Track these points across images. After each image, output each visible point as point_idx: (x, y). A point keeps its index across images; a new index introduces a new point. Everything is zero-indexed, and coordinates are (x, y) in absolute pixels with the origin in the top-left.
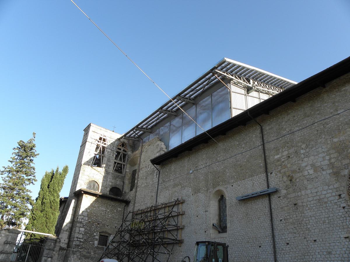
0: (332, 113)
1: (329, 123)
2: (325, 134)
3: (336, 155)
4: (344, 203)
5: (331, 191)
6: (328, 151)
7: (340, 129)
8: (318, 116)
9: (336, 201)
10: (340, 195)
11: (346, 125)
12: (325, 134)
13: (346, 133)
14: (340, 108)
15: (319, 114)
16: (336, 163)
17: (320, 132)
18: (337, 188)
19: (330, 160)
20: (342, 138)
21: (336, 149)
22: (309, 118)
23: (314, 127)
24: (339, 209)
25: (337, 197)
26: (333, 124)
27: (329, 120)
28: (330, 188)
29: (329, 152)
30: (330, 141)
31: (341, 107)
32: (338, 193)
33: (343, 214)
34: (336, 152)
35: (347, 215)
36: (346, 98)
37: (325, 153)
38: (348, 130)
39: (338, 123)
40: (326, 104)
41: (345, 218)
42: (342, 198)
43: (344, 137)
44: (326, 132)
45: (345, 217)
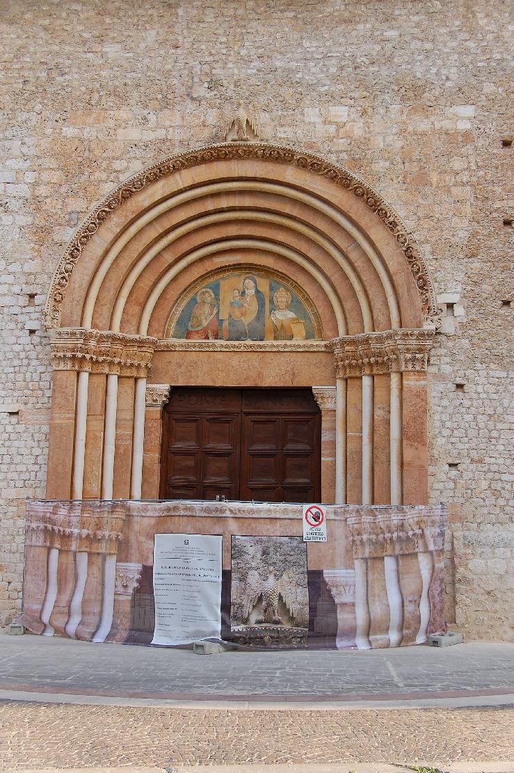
0: (85, 42)
3: (56, 177)
5: (10, 279)
8: (42, 34)
9: (16, 310)
10: (32, 296)
11: (112, 98)
13: (104, 122)
14: (114, 38)
15: (45, 29)
16: (48, 201)
17: (34, 89)
18: (30, 274)
19: (35, 184)
20: (90, 133)
22: (13, 28)
23: (18, 66)
24: (17, 332)
25: (23, 300)
28: (12, 268)
29: (40, 162)
31: (115, 35)
32: (29, 290)
34: (58, 169)
35: (33, 355)
36: (140, 12)
37: (28, 161)
40: (79, 8)
41: (25, 362)
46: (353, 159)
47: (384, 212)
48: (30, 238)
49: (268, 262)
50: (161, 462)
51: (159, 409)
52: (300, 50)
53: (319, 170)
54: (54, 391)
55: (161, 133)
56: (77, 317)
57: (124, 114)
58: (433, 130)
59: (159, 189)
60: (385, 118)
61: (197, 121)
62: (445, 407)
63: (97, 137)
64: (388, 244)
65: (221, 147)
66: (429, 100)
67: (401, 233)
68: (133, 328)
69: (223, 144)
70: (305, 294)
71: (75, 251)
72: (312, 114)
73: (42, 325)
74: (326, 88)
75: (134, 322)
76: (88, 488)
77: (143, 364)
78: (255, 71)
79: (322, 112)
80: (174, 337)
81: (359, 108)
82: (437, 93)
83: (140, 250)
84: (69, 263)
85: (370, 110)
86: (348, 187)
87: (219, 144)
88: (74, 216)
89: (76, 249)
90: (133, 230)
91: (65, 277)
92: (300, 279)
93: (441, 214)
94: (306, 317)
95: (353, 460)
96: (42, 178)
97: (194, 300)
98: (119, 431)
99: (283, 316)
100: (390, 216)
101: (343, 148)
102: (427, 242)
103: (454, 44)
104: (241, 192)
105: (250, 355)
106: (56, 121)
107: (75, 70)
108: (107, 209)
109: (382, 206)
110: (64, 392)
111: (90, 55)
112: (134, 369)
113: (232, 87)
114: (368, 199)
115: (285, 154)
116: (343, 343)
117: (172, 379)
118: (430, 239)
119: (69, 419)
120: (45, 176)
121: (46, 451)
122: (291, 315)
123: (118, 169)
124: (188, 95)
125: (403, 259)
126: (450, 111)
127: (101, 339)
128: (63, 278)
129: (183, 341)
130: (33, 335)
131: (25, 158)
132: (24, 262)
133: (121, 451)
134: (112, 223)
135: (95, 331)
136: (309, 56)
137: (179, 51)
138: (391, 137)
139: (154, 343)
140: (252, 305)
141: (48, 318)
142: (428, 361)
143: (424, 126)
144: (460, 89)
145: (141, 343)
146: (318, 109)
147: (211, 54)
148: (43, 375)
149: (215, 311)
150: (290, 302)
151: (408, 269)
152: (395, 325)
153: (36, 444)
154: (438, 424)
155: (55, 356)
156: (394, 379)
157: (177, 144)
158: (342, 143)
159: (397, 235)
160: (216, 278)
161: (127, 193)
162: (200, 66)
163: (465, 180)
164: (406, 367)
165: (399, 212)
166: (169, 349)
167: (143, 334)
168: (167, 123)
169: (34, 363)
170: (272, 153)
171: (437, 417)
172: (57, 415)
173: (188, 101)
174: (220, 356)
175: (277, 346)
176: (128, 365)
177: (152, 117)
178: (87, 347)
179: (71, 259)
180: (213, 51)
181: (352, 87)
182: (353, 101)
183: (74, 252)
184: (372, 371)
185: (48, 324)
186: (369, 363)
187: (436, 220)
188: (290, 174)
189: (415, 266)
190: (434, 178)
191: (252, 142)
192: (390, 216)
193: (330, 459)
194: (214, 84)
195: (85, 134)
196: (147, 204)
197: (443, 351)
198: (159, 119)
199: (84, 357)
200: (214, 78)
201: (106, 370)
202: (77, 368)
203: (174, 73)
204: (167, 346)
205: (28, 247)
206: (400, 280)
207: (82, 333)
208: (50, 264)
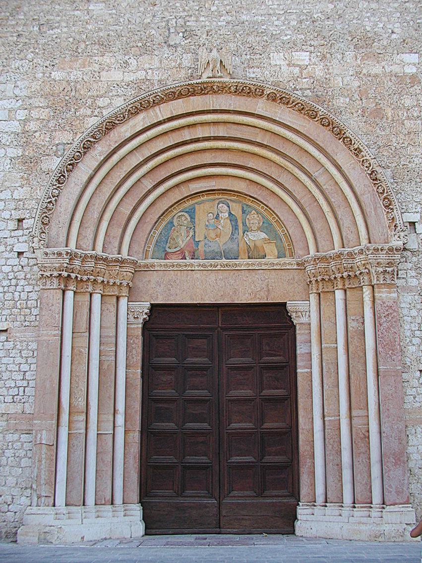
1: (57, 25)
2: (37, 51)
3: (45, 114)
6: (30, 98)
7: (80, 51)
10: (20, 221)
11: (97, 47)
12: (37, 51)
16: (37, 134)
17: (27, 41)
19: (26, 121)
20: (76, 75)
21: (52, 98)
25: (12, 225)
26: (65, 33)
27: (59, 18)
29: (31, 101)
30: (44, 73)
32: (17, 215)
37: (20, 101)
38: (96, 58)
39: (80, 33)
41: (14, 282)
43: (81, 73)
44: (40, 46)
45: (15, 278)
46: (317, 96)
47: (349, 139)
48: (20, 168)
49: (241, 186)
50: (142, 377)
51: (140, 326)
52: (263, 7)
53: (288, 103)
54: (41, 309)
55: (141, 75)
56: (62, 239)
57: (107, 59)
58: (385, 74)
59: (140, 121)
60: (341, 62)
61: (174, 64)
62: (414, 318)
63: (83, 79)
64: (354, 168)
65: (197, 83)
66: (379, 48)
67: (365, 158)
68: (115, 250)
69: (199, 81)
70: (275, 216)
71: (62, 177)
72: (278, 59)
74: (289, 37)
75: (117, 244)
76: (75, 403)
77: (125, 284)
78: (224, 23)
79: (286, 57)
81: (319, 54)
82: (385, 43)
83: (122, 177)
84: (56, 189)
85: (328, 55)
86: (315, 118)
87: (195, 82)
88: (61, 147)
89: (62, 175)
90: (116, 158)
91: (52, 201)
92: (272, 203)
93: (398, 144)
94: (276, 237)
95: (328, 370)
96: (32, 115)
97: (171, 223)
98: (102, 347)
99: (257, 237)
100: (354, 144)
101: (307, 86)
102: (388, 167)
103: (396, 5)
104: (216, 123)
105: (226, 274)
106: (46, 67)
107: (64, 24)
108: (92, 140)
109: (347, 134)
110: (50, 310)
111: (76, 13)
112: (116, 287)
113: (204, 36)
114: (334, 128)
115: (256, 90)
116: (317, 259)
117: (152, 297)
118: (390, 165)
119: (54, 336)
120: (35, 114)
121: (33, 367)
122: (263, 235)
123: (102, 106)
124: (165, 43)
125: (368, 181)
126: (397, 58)
127: (84, 258)
128: (51, 202)
129: (163, 262)
130: (21, 256)
131: (18, 98)
132: (14, 190)
133: (105, 367)
134: (96, 152)
135: (79, 252)
136: (271, 12)
137: (156, 8)
138: (348, 78)
139: (135, 263)
140: (225, 225)
141: (36, 240)
142: (397, 275)
143: (377, 70)
144: (404, 41)
145: (123, 261)
146: (283, 54)
147: (184, 10)
149: (191, 234)
150: (261, 223)
151: (373, 190)
152: (364, 242)
153: (24, 361)
154: (408, 333)
155: (42, 275)
156: (367, 292)
157: (156, 83)
158: (305, 83)
159: (362, 160)
160: (191, 202)
161: (110, 126)
162: (175, 20)
163: (415, 115)
164: (378, 280)
165: (361, 141)
166: (148, 268)
167: (125, 254)
168: (147, 66)
169: (22, 282)
170: (244, 88)
171: (407, 327)
172: (45, 332)
173: (166, 48)
174: (198, 275)
175: (253, 264)
177: (133, 62)
178: (72, 266)
179: (58, 185)
180: (187, 8)
181: (312, 37)
182: (313, 48)
183: (61, 179)
184: (344, 285)
185: (35, 245)
186: (342, 277)
187: (393, 149)
188: (261, 106)
189: (380, 187)
190: (389, 113)
191: (226, 79)
192: (354, 144)
193: (306, 370)
194: (188, 34)
195: (72, 77)
196: (128, 135)
197: (409, 265)
198: (139, 63)
199: (69, 276)
200: (188, 29)
201: (90, 290)
203: (153, 25)
204: (146, 266)
205: (18, 176)
206: (366, 199)
207: (67, 253)
208: (38, 191)
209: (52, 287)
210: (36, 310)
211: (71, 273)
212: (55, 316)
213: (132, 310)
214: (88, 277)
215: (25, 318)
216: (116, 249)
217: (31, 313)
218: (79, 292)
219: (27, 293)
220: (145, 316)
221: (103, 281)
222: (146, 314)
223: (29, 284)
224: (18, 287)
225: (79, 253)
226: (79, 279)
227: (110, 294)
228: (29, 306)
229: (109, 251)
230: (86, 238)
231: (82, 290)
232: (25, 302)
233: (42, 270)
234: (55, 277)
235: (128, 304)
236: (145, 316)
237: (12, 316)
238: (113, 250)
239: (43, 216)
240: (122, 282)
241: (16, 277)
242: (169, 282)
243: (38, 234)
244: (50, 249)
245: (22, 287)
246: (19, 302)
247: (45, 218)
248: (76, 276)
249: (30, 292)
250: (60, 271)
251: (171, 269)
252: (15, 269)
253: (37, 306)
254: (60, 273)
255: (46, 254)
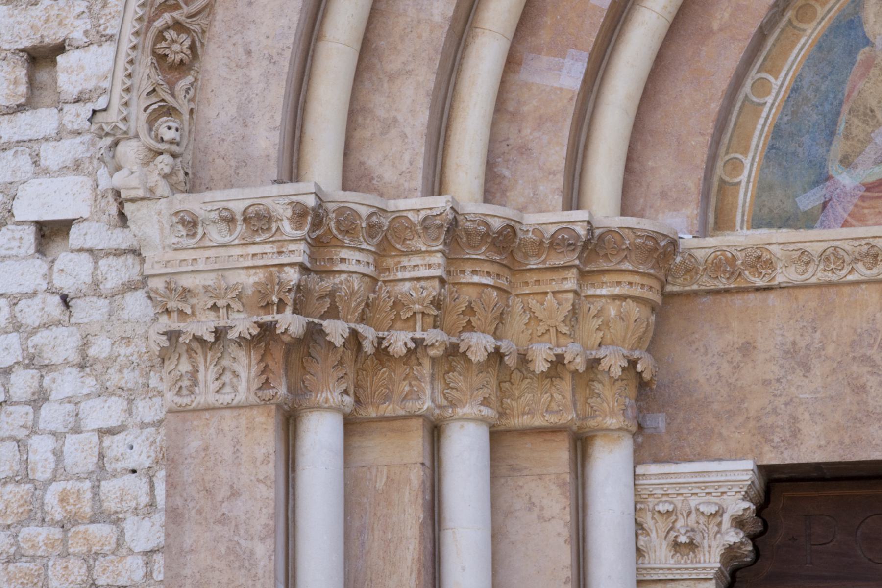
4: (77, 166)
33: (17, 327)
42: (59, 104)
45: (31, 361)
54: (174, 516)
73: (98, 196)
80: (757, 223)
110: (223, 520)
112: (566, 386)
117: (764, 433)
141: (129, 151)
148: (116, 445)
155: (173, 336)
176: (541, 366)
178: (328, 283)
199: (314, 333)
202: (282, 390)
209: (226, 398)
210: (147, 523)
211: (323, 317)
212: (252, 553)
213: (662, 508)
214: (419, 335)
215: (90, 569)
216: (559, 181)
217: (118, 545)
218: (371, 420)
219: (95, 438)
220: (734, 537)
221: (497, 355)
222: (739, 523)
223: (104, 392)
224: (46, 410)
225: (364, 211)
226: (368, 348)
227: (538, 422)
228: (111, 505)
229: (519, 193)
230: (394, 133)
231: (388, 409)
232: (87, 484)
233: (168, 312)
234: (241, 341)
235: (635, 476)
236: (734, 537)
237: (23, 565)
238: (542, 188)
239: (159, 24)
240: (601, 353)
241: (32, 358)
242: (853, 344)
243: (138, 118)
244: (208, 196)
245: (69, 407)
246: (56, 488)
247: (171, 34)
248: (354, 333)
249: (111, 432)
250: (267, 307)
251: (862, 272)
252: (30, 313)
253: (152, 504)
254: (268, 318)
255: (191, 224)
